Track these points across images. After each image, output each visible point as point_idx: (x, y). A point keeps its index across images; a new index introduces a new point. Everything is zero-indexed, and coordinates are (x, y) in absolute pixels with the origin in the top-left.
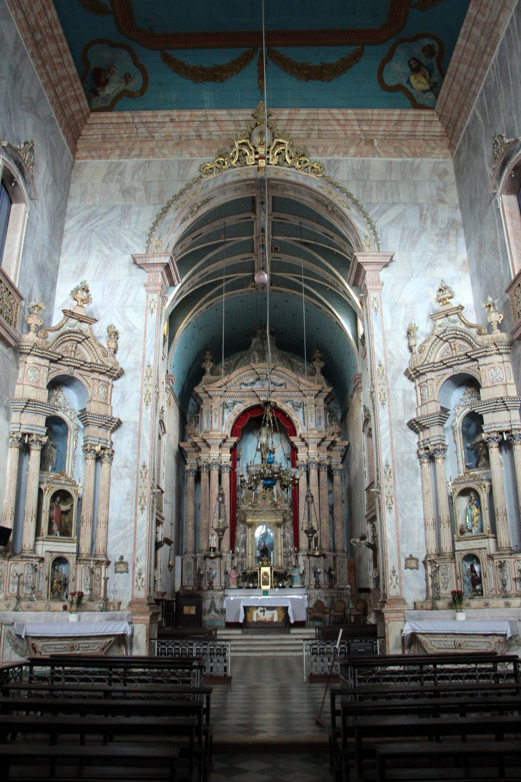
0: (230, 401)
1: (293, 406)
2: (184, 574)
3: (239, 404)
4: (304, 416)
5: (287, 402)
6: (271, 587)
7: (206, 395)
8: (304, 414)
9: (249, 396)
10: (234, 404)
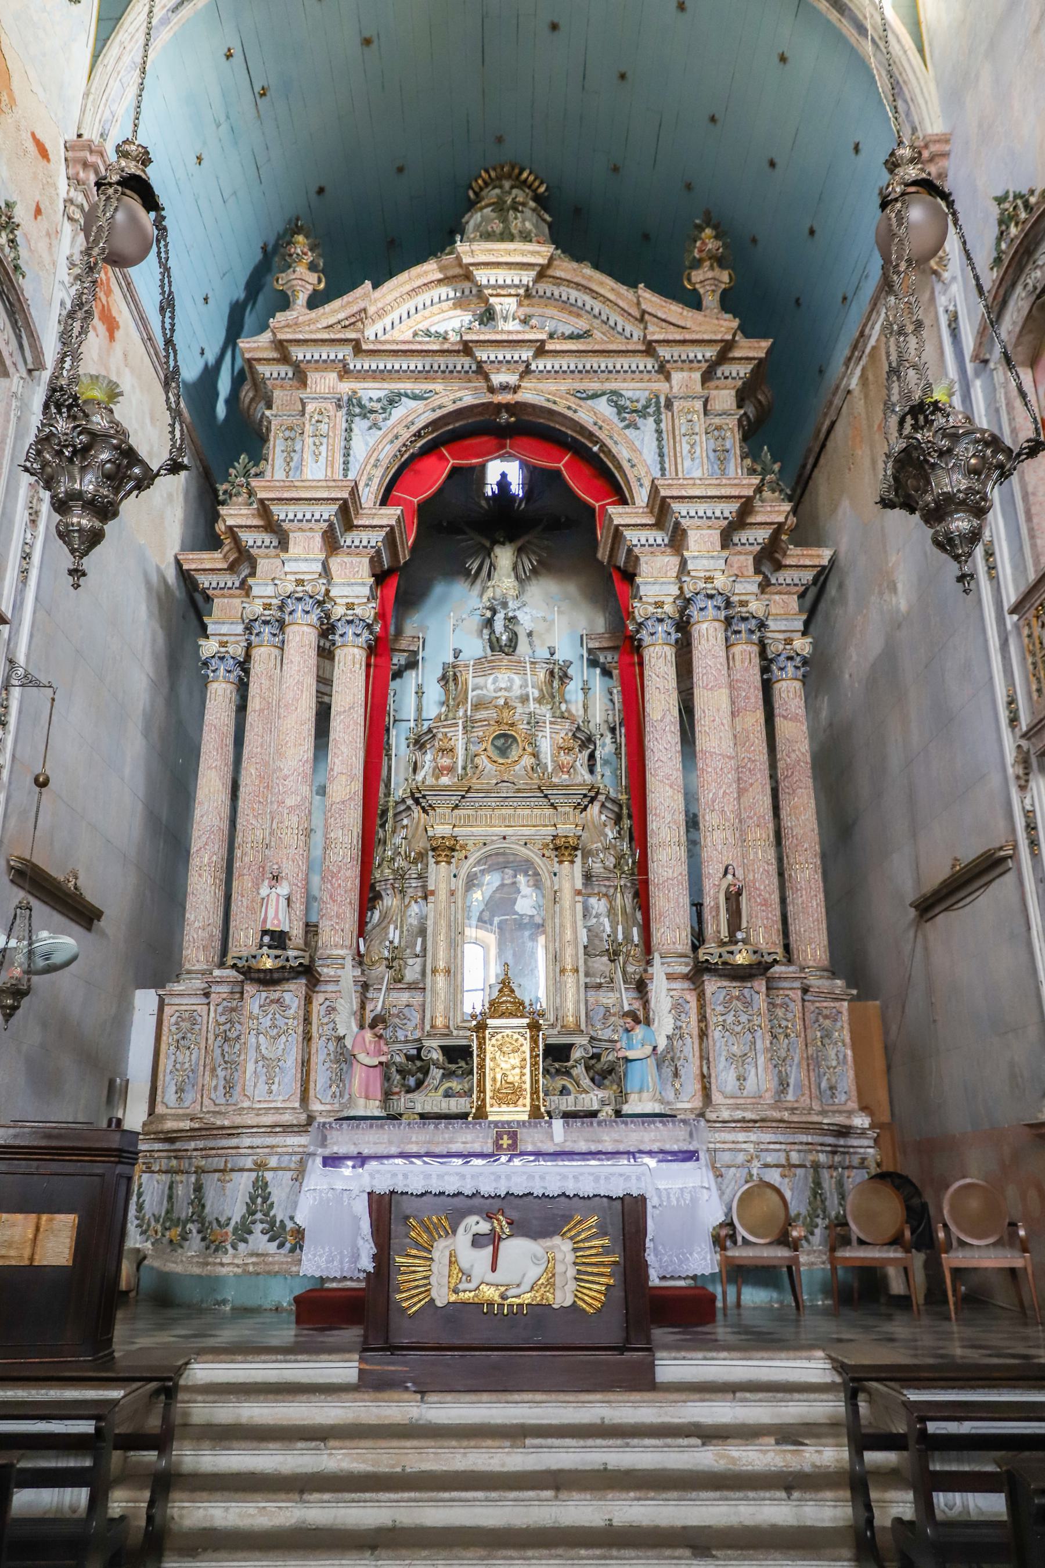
0: (376, 394)
1: (621, 410)
2: (166, 1064)
3: (413, 404)
4: (660, 448)
5: (595, 396)
6: (535, 1113)
7: (286, 370)
8: (659, 439)
9: (448, 374)
10: (393, 400)
